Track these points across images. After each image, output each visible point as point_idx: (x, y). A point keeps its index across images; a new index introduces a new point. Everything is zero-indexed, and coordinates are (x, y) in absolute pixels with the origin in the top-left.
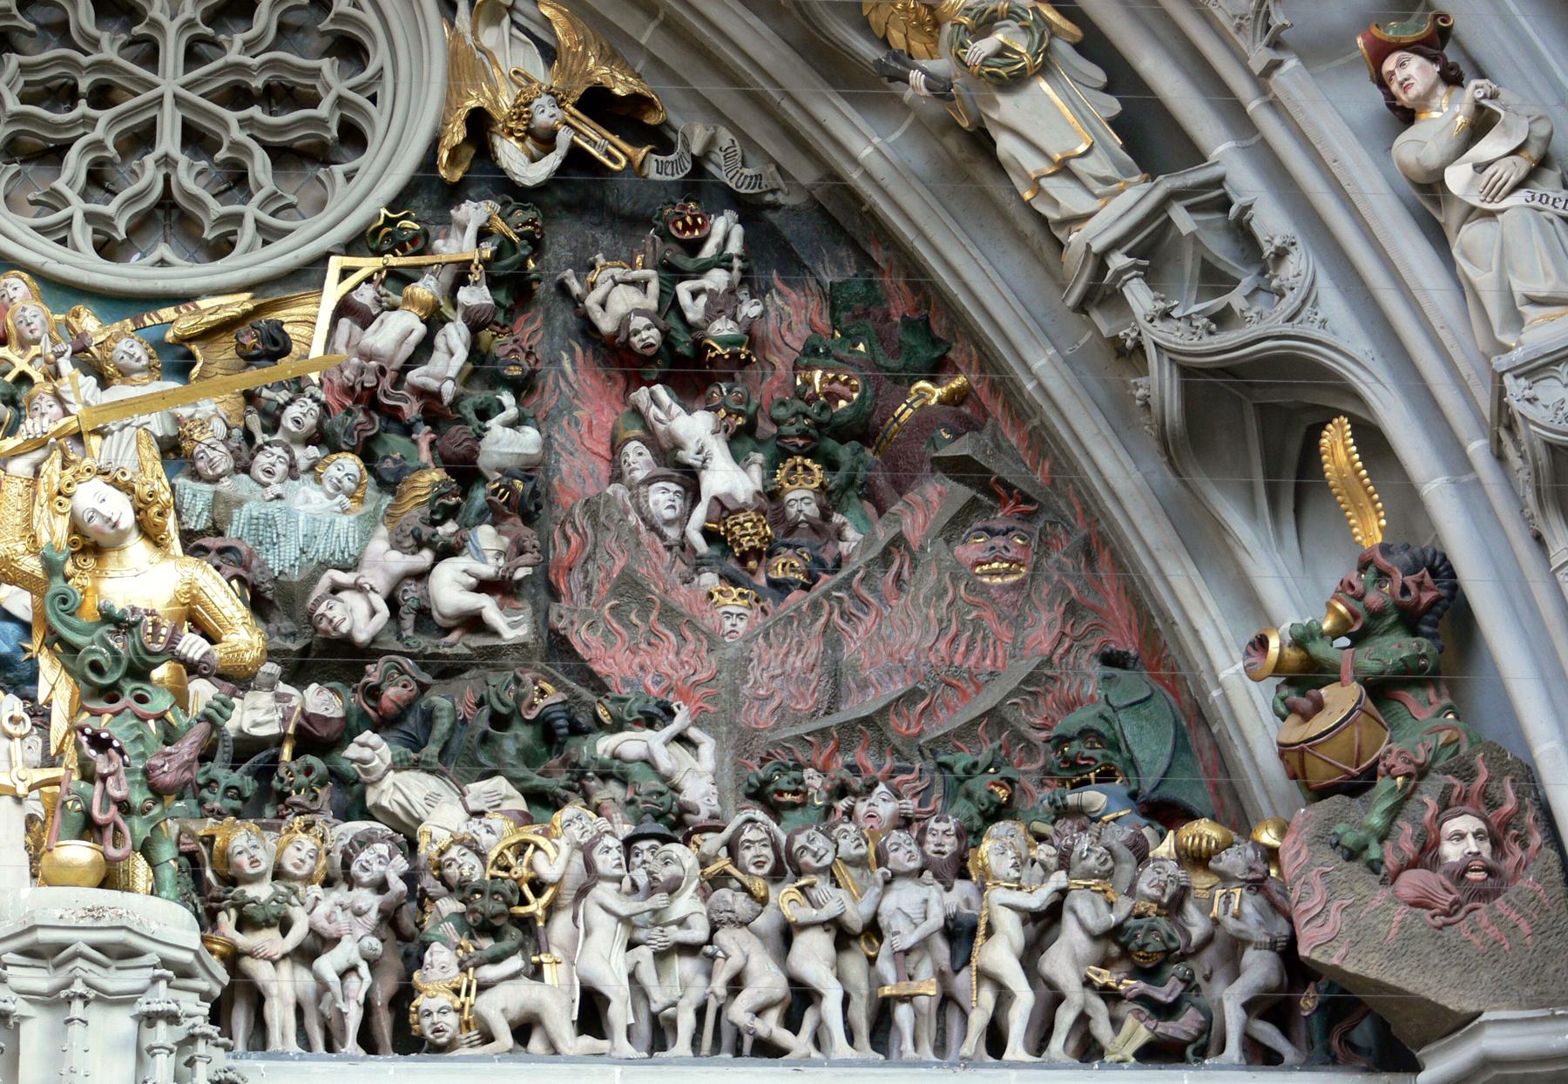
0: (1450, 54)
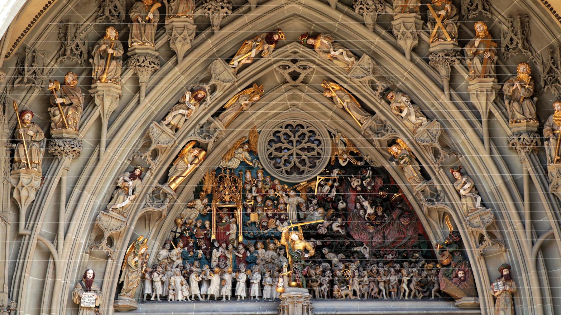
0: (462, 171)
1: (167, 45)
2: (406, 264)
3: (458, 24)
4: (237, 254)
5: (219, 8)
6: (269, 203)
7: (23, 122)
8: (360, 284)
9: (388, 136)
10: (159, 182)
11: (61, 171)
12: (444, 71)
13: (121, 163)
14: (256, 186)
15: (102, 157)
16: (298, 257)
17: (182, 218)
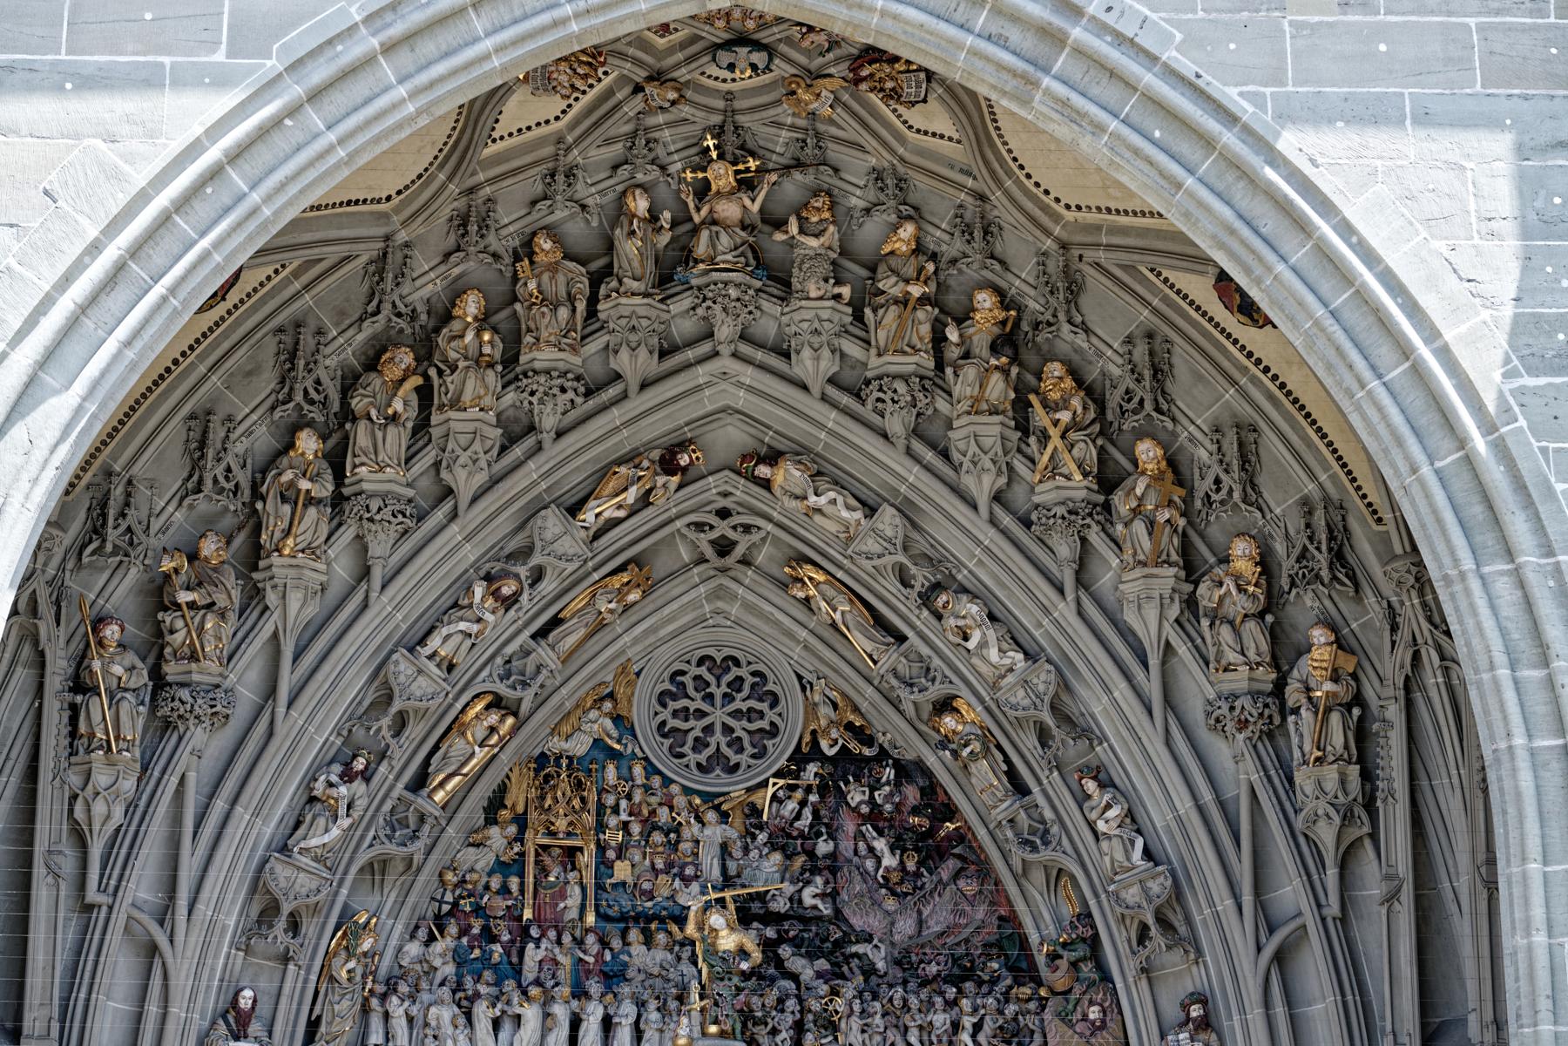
0: (1101, 776)
1: (432, 472)
2: (969, 986)
3: (1100, 442)
5: (556, 391)
6: (657, 837)
7: (100, 644)
8: (863, 1031)
9: (936, 691)
10: (406, 788)
11: (184, 759)
12: (1065, 548)
13: (321, 741)
15: (280, 728)
16: (724, 966)
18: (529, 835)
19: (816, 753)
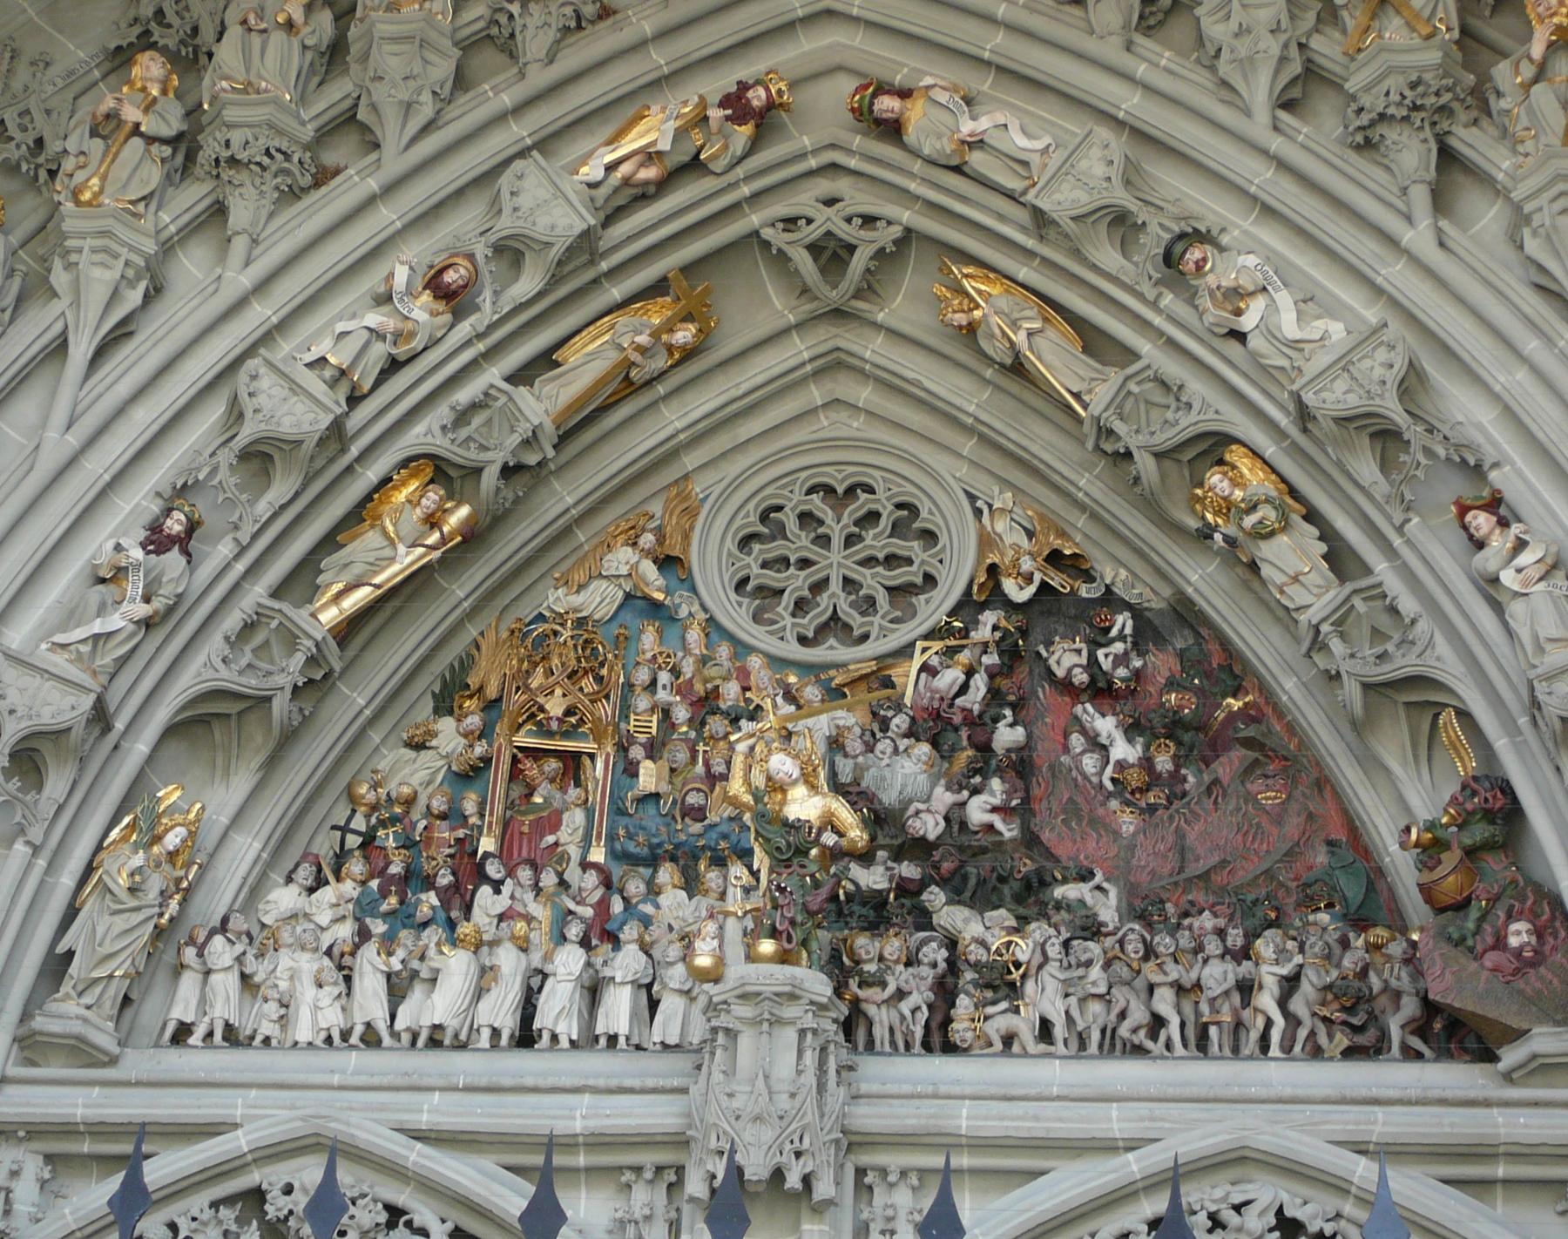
0: (1503, 511)
4: (572, 905)
14: (676, 672)
17: (375, 786)
18: (501, 728)
19: (995, 596)
